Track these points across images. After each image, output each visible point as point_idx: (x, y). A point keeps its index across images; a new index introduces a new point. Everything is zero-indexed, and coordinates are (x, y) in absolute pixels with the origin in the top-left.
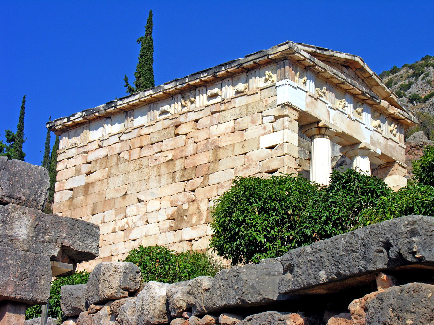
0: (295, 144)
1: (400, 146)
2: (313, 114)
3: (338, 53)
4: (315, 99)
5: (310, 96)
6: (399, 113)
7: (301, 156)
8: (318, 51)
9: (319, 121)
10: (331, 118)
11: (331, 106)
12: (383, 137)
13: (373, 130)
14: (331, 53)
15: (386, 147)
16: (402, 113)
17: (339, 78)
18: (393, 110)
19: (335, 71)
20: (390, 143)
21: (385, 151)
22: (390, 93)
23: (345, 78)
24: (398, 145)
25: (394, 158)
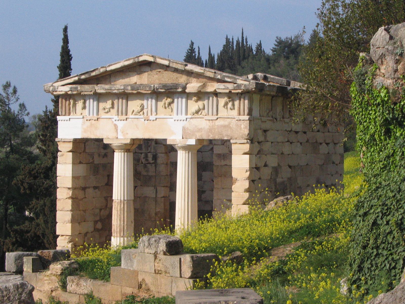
3: (112, 65)
4: (95, 120)
5: (87, 120)
10: (119, 131)
11: (117, 119)
15: (210, 130)
16: (224, 88)
17: (114, 91)
19: (107, 87)
21: (209, 136)
22: (202, 71)
23: (122, 87)
24: (234, 120)
25: (225, 138)
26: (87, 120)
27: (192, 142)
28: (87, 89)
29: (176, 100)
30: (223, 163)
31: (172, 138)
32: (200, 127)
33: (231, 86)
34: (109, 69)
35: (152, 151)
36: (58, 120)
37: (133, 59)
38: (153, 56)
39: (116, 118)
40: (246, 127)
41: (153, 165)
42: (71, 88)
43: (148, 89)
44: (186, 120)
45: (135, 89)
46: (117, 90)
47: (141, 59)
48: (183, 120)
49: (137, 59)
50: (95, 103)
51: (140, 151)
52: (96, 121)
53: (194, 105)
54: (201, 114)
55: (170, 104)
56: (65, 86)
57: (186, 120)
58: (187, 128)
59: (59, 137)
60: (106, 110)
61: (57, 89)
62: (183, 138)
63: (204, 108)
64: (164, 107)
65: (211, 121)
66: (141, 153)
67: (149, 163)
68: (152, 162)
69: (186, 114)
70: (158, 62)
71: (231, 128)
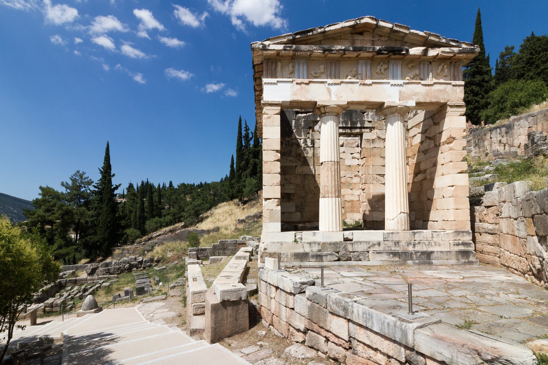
1: (454, 86)
2: (303, 99)
5: (297, 84)
6: (443, 52)
7: (374, 120)
9: (316, 102)
10: (332, 94)
12: (423, 85)
14: (319, 31)
15: (427, 94)
18: (432, 53)
20: (437, 87)
21: (426, 99)
23: (343, 48)
25: (442, 101)
26: (297, 84)
27: (412, 103)
29: (391, 66)
30: (372, 146)
31: (391, 100)
32: (416, 91)
33: (456, 50)
35: (310, 137)
36: (263, 83)
39: (330, 81)
40: (461, 92)
41: (312, 148)
42: (284, 47)
46: (337, 50)
50: (305, 67)
51: (299, 138)
52: (307, 86)
55: (385, 69)
58: (404, 92)
59: (264, 99)
60: (318, 75)
62: (400, 100)
64: (379, 72)
65: (427, 87)
66: (300, 139)
67: (308, 147)
68: (310, 146)
71: (446, 92)
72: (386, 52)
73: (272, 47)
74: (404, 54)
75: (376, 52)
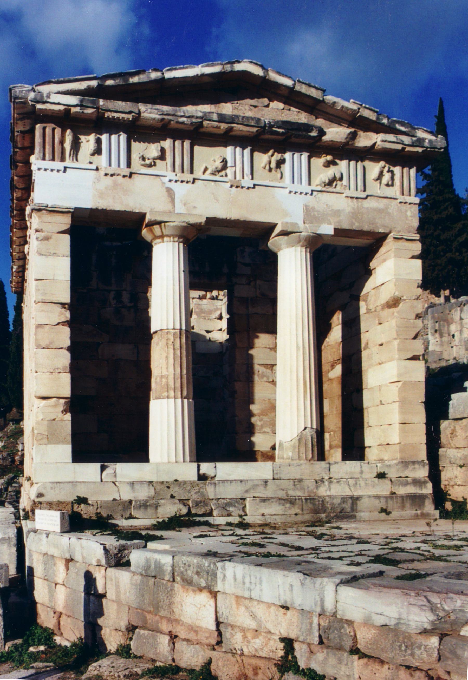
0: (60, 278)
3: (175, 69)
8: (110, 82)
13: (312, 191)
14: (154, 75)
19: (166, 108)
23: (200, 114)
28: (119, 109)
34: (169, 75)
37: (221, 64)
38: (262, 66)
42: (81, 101)
43: (253, 124)
44: (312, 194)
45: (227, 121)
47: (238, 67)
48: (306, 194)
49: (229, 66)
53: (321, 171)
54: (335, 187)
56: (68, 97)
57: (312, 194)
61: (48, 97)
63: (341, 179)
69: (310, 184)
70: (272, 80)
72: (281, 131)
73: (55, 98)
74: (314, 137)
75: (261, 127)
